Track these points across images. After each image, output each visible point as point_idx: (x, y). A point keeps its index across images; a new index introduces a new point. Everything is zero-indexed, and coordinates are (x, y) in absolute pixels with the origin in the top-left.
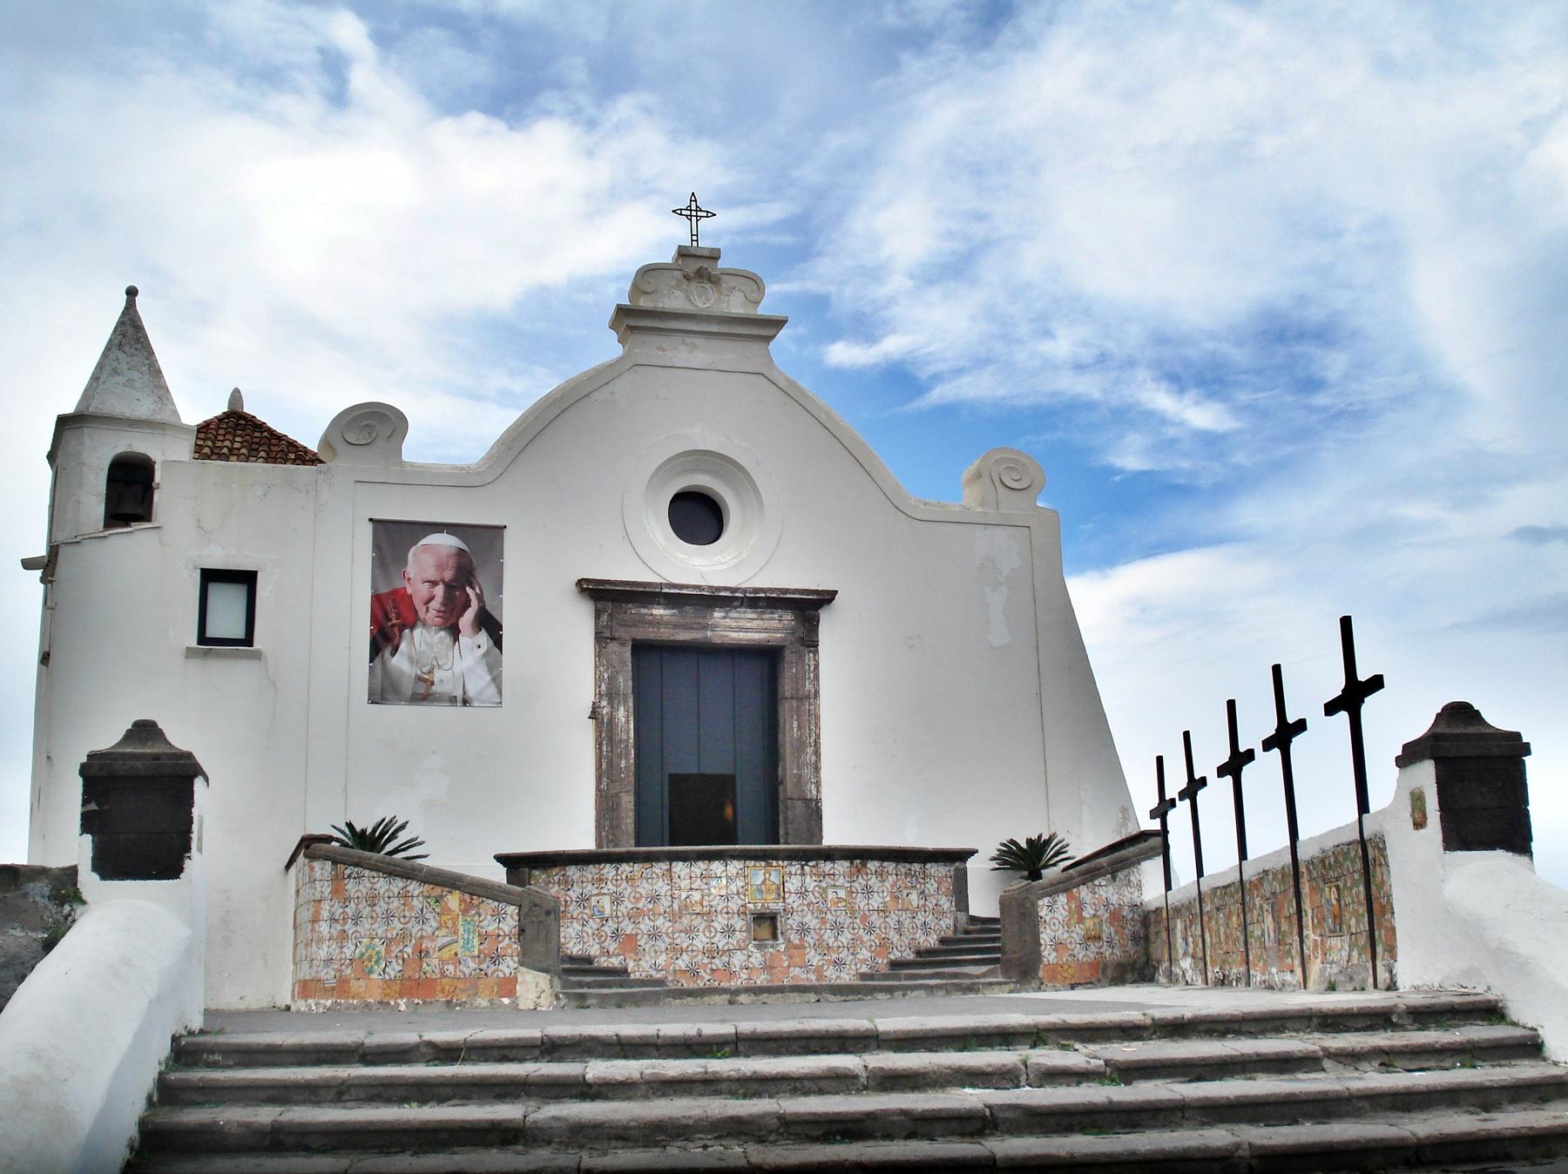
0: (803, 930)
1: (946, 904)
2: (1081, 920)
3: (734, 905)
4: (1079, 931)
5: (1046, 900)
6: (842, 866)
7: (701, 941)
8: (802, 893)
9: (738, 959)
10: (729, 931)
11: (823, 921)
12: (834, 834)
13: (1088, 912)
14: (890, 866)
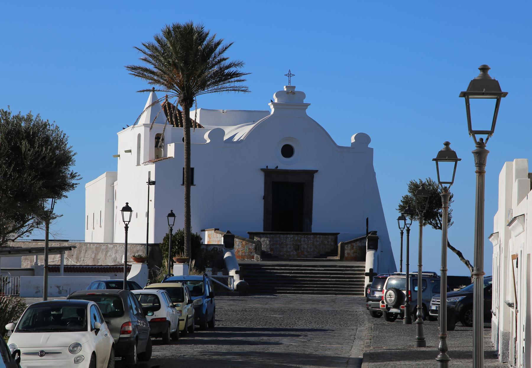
0: (304, 248)
1: (332, 243)
7: (285, 250)
8: (304, 241)
9: (292, 253)
10: (290, 248)
12: (313, 231)
14: (321, 236)
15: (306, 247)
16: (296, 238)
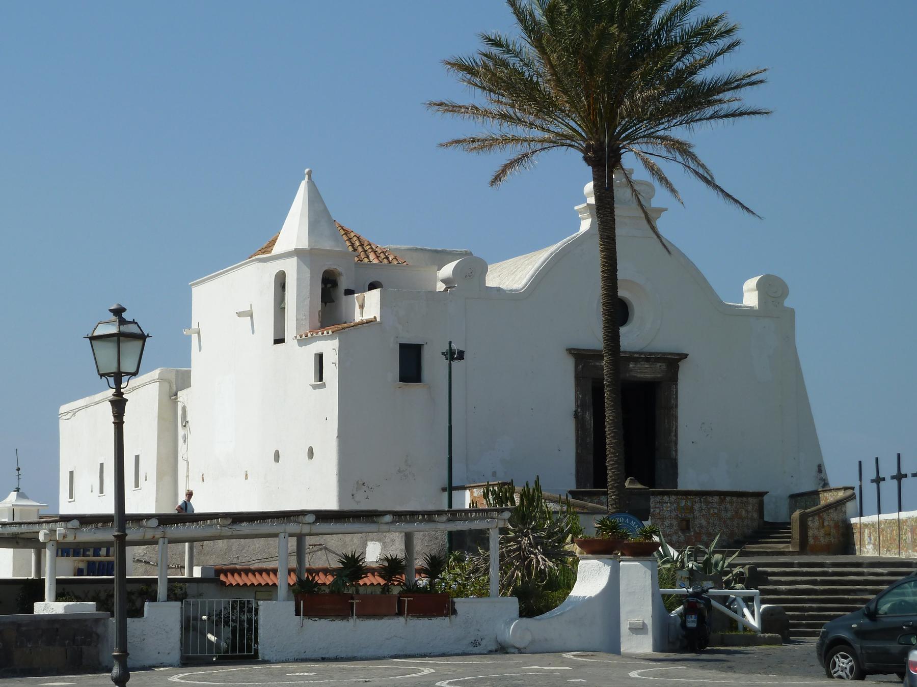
0: (701, 527)
2: (823, 526)
3: (673, 514)
4: (822, 532)
5: (810, 519)
6: (716, 499)
8: (701, 510)
11: (709, 523)
13: (826, 523)
14: (735, 499)
15: (704, 522)
16: (683, 504)
